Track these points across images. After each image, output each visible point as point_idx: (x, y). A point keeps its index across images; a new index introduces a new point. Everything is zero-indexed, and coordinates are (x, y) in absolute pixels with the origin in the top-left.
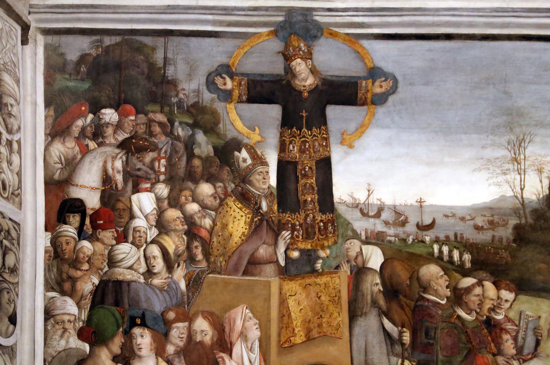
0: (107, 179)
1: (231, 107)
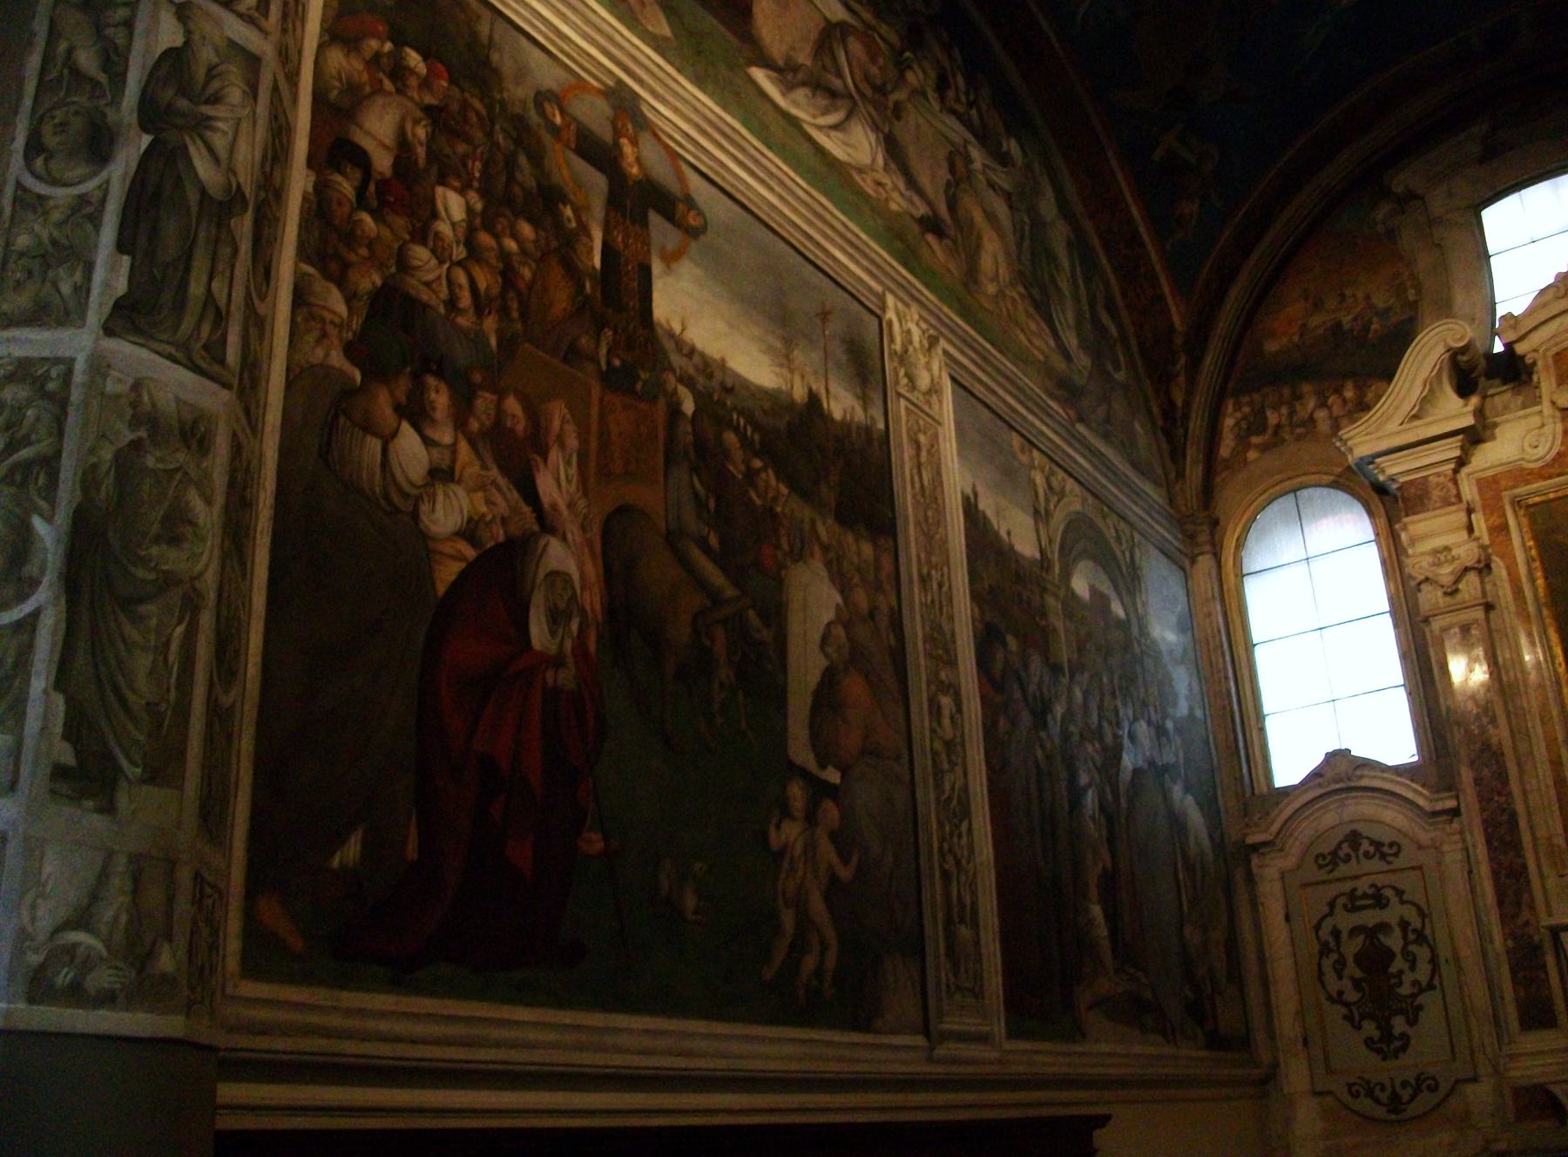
0: (403, 145)
1: (558, 146)
